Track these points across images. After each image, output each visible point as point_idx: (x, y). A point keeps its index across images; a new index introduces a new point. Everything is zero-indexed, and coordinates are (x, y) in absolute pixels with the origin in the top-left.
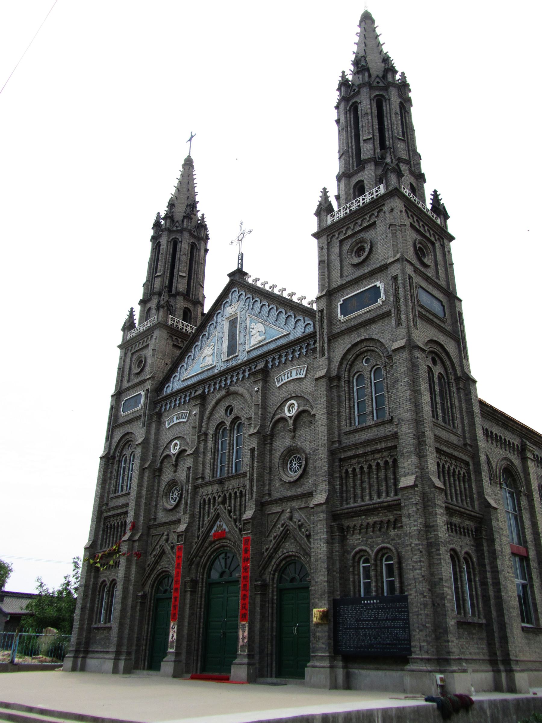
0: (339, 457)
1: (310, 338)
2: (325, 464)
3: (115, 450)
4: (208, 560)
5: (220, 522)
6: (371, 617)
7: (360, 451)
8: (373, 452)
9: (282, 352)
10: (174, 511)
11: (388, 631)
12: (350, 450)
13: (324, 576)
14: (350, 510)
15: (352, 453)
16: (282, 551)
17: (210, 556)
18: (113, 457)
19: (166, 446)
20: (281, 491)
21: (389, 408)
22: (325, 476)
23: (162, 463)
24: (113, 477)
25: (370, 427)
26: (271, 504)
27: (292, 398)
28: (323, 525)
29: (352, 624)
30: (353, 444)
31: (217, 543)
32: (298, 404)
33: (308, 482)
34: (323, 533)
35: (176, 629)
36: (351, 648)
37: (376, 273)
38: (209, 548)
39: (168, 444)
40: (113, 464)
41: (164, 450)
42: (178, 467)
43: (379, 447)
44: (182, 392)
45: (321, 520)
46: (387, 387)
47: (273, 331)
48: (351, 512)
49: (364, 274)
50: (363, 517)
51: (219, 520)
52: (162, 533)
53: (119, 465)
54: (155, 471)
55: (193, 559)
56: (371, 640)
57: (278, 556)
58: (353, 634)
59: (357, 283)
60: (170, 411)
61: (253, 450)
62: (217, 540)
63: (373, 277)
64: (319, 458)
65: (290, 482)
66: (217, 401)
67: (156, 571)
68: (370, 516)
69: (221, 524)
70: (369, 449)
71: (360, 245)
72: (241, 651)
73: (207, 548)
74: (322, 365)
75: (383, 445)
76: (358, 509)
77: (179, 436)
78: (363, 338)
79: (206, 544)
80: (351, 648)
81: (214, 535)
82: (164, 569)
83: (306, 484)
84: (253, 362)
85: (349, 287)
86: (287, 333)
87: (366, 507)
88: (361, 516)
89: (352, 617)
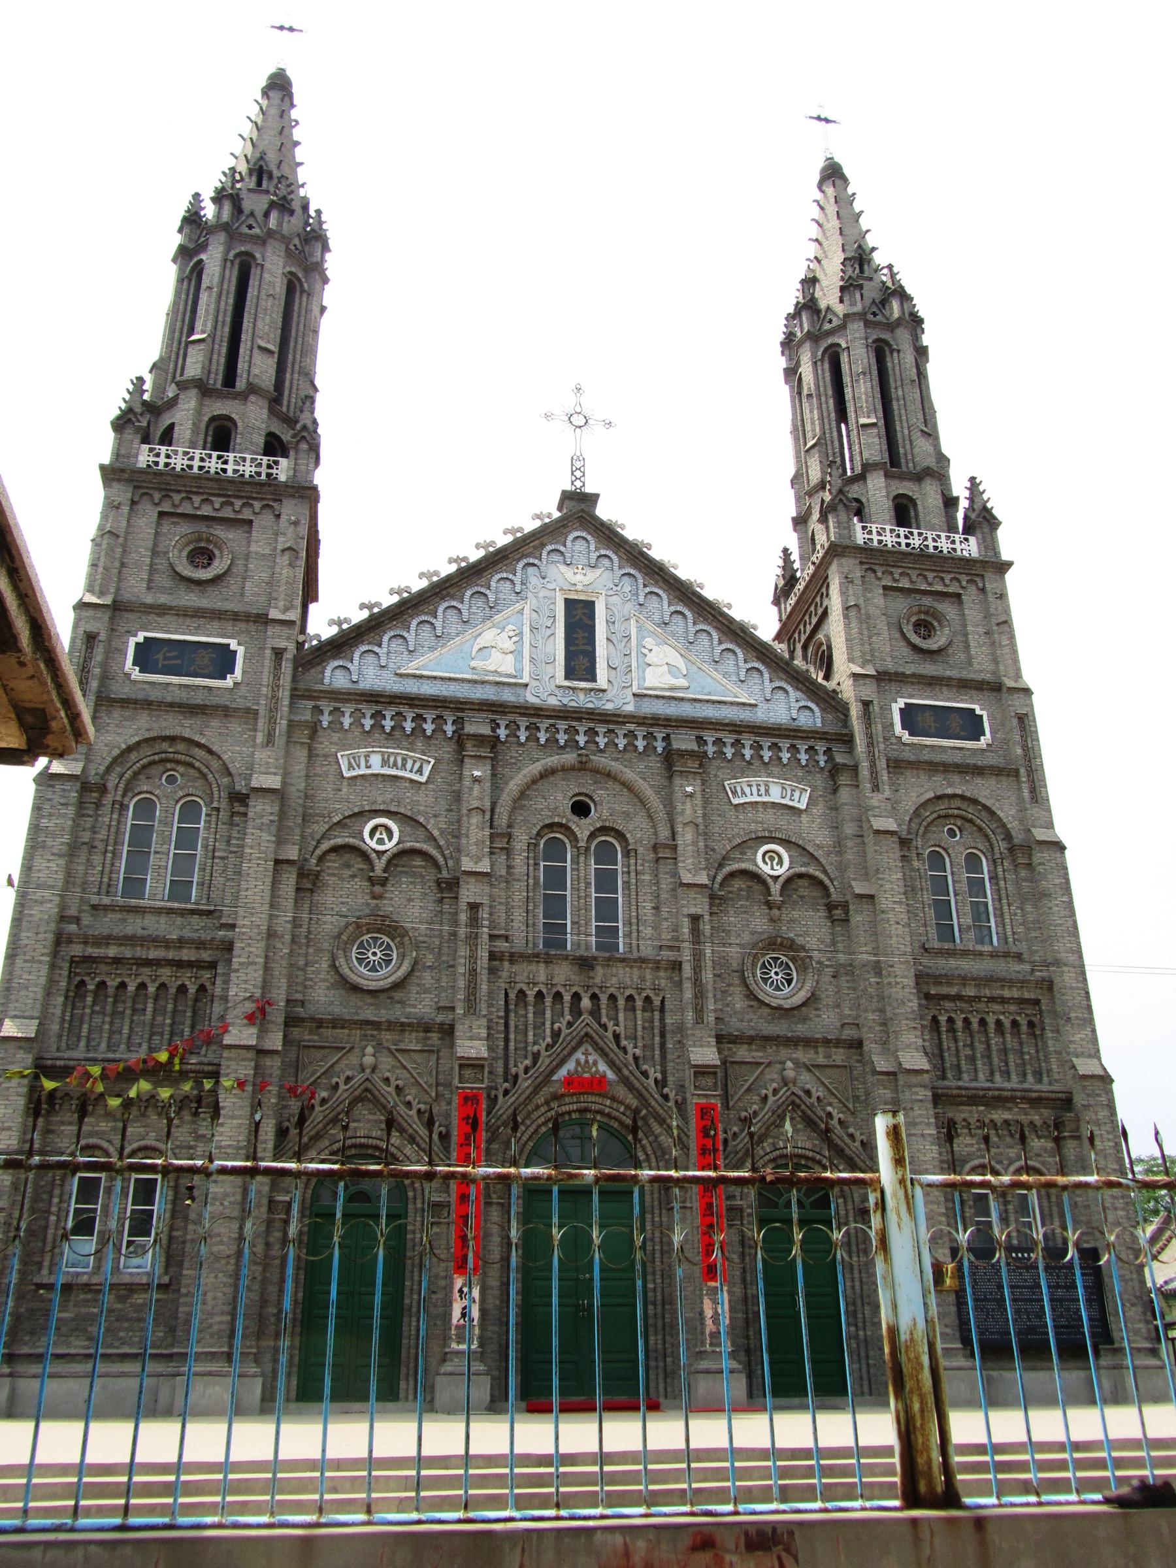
0: (925, 991)
1: (820, 739)
2: (912, 997)
3: (109, 769)
4: (530, 1138)
5: (586, 1054)
6: (1026, 1281)
7: (970, 992)
8: (992, 999)
9: (745, 736)
10: (382, 996)
11: (1062, 1306)
12: (949, 984)
13: (939, 1203)
14: (964, 1092)
15: (953, 991)
16: (773, 1144)
17: (539, 1126)
18: (103, 790)
19: (339, 822)
20: (751, 1021)
21: (1014, 933)
22: (915, 1019)
23: (321, 859)
24: (101, 846)
25: (981, 954)
26: (734, 1042)
27: (785, 843)
28: (927, 1109)
29: (991, 1293)
30: (960, 976)
31: (567, 1100)
32: (790, 856)
33: (819, 1016)
34: (928, 1124)
35: (476, 1293)
36: (993, 1333)
37: (970, 688)
38: (543, 1110)
39: (345, 818)
40: (98, 805)
41: (330, 828)
42: (389, 887)
43: (1007, 993)
44: (412, 706)
45: (921, 1101)
46: (1007, 896)
47: (709, 680)
48: (962, 1096)
49: (950, 678)
50: (982, 1108)
51: (582, 1049)
52: (348, 1046)
53: (120, 814)
54: (302, 875)
55: (499, 1127)
56: (1030, 1320)
57: (762, 1153)
58: (993, 1310)
59: (930, 684)
60: (349, 735)
61: (695, 919)
62: (572, 1095)
63: (963, 691)
64: (897, 983)
65: (779, 1008)
66: (546, 770)
67: (327, 1143)
68: (995, 1108)
69: (591, 1059)
70: (987, 992)
71: (922, 617)
72: (711, 1345)
73: (537, 1107)
74: (878, 807)
75: (1016, 993)
76: (981, 1093)
77: (393, 809)
78: (959, 792)
79: (540, 1099)
80: (993, 1333)
81: (569, 1081)
82: (363, 1140)
83: (817, 1019)
84: (665, 726)
85: (913, 683)
86: (753, 702)
87: (996, 1093)
88: (976, 1105)
89: (989, 1280)
